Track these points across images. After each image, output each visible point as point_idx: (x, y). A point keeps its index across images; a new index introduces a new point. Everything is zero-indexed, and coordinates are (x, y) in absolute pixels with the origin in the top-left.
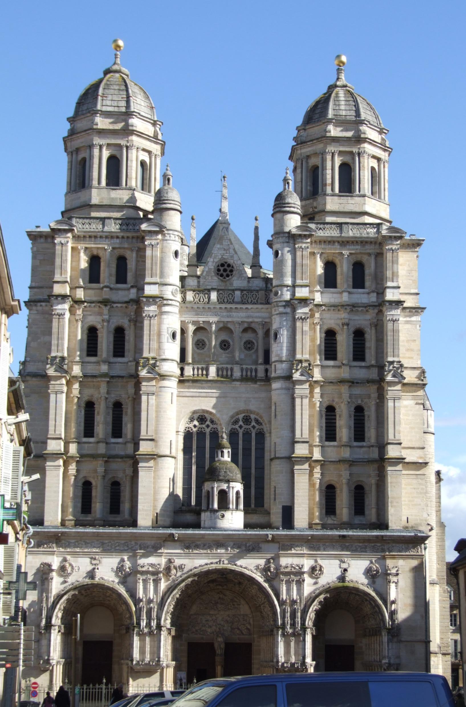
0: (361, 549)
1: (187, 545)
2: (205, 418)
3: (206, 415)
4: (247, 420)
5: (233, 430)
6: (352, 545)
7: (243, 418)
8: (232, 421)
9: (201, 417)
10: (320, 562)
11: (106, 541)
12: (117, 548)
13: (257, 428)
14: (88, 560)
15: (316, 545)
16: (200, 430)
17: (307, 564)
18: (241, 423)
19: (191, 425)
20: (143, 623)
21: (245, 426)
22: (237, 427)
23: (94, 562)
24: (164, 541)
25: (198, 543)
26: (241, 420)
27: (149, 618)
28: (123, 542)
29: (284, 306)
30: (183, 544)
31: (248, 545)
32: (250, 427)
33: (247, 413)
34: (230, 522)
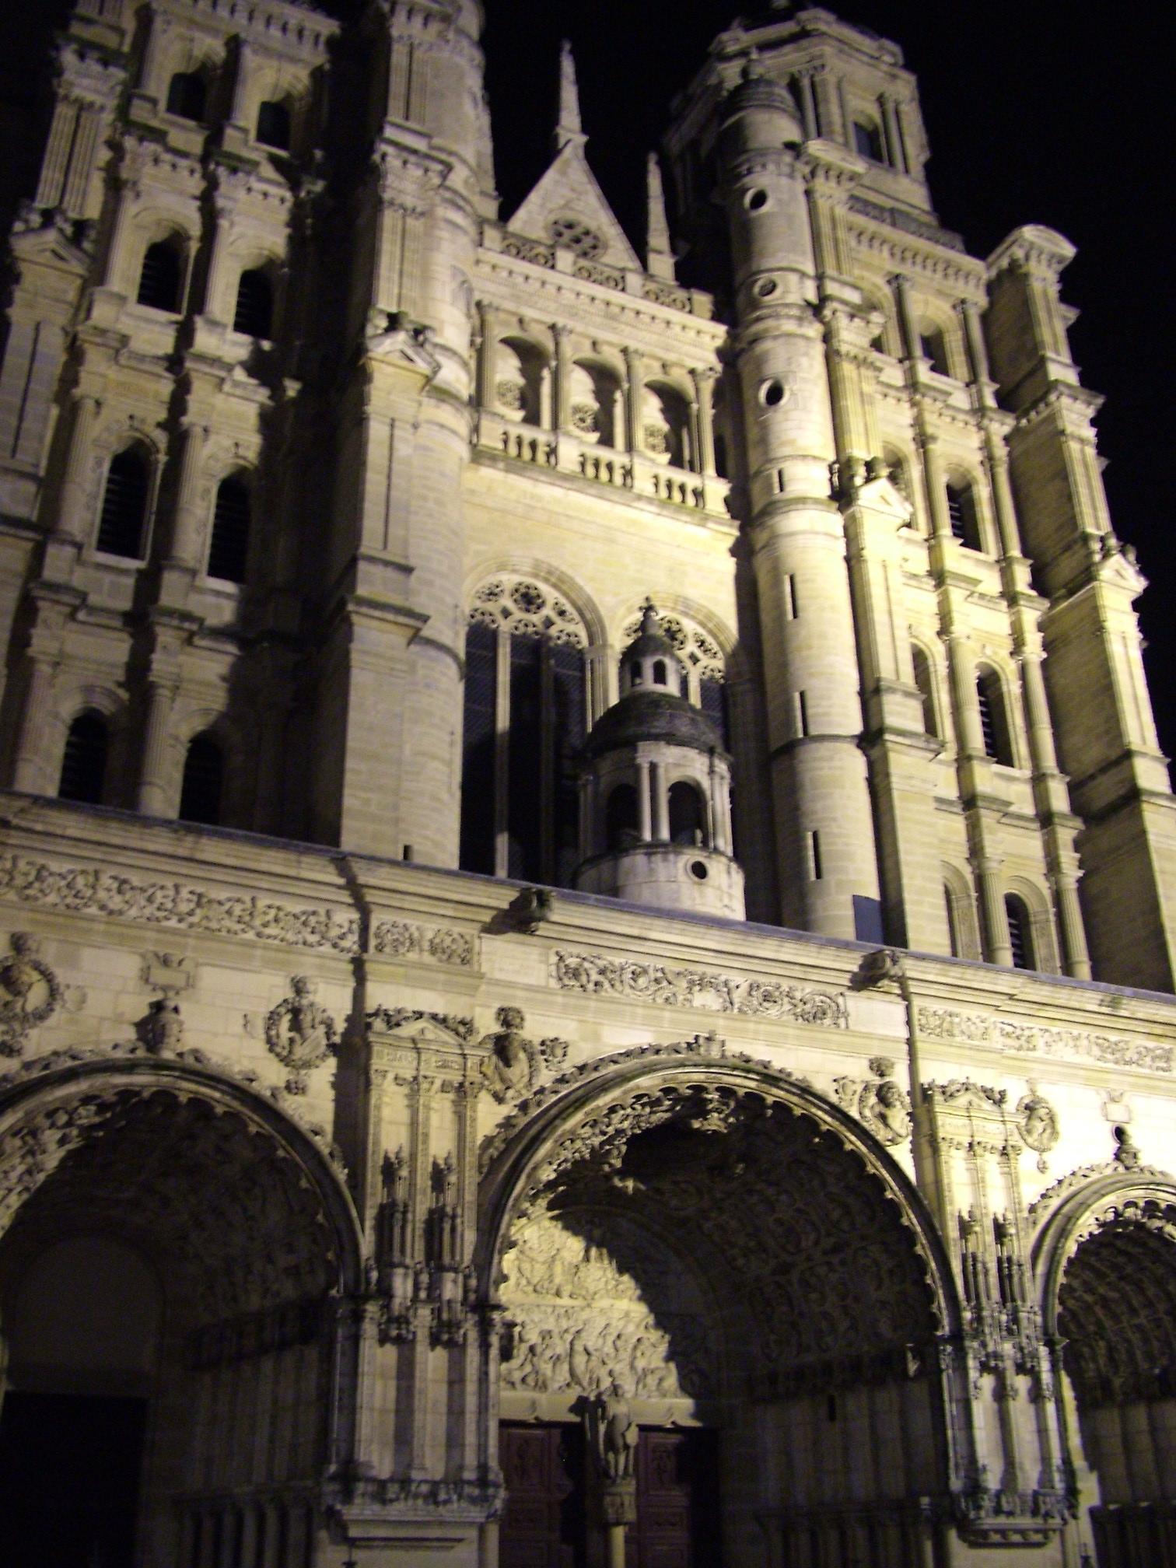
0: (1153, 1059)
1: (572, 962)
2: (539, 596)
3: (545, 589)
6: (1127, 1042)
9: (523, 590)
10: (1042, 1092)
11: (223, 894)
12: (272, 930)
14: (127, 965)
16: (521, 626)
19: (490, 606)
20: (402, 1286)
23: (160, 975)
25: (618, 960)
27: (435, 1261)
28: (297, 907)
29: (800, 319)
30: (554, 959)
33: (673, 609)
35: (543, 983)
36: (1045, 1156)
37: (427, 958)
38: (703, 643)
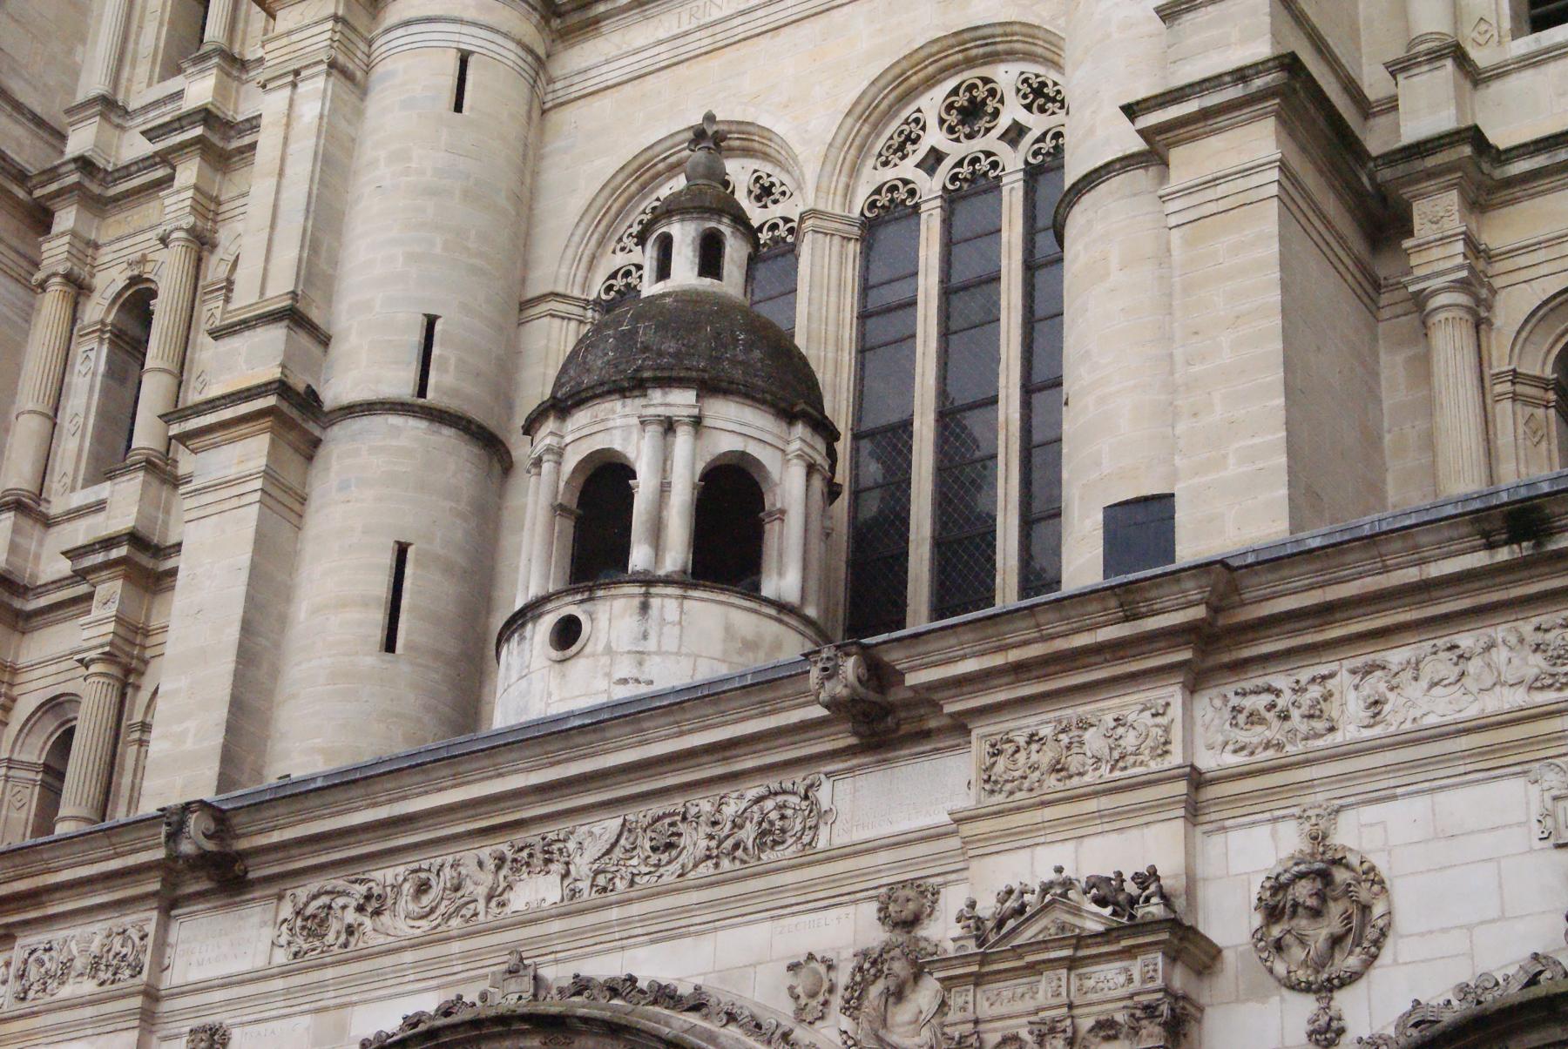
4: (971, 112)
5: (884, 199)
7: (950, 107)
8: (880, 144)
13: (1036, 133)
15: (1299, 690)
17: (1228, 878)
18: (934, 137)
21: (956, 150)
22: (907, 168)
24: (169, 905)
26: (932, 123)
31: (730, 810)
32: (991, 141)
33: (970, 63)
34: (625, 669)
35: (260, 962)
36: (1343, 1000)
37: (89, 987)
38: (1039, 91)
